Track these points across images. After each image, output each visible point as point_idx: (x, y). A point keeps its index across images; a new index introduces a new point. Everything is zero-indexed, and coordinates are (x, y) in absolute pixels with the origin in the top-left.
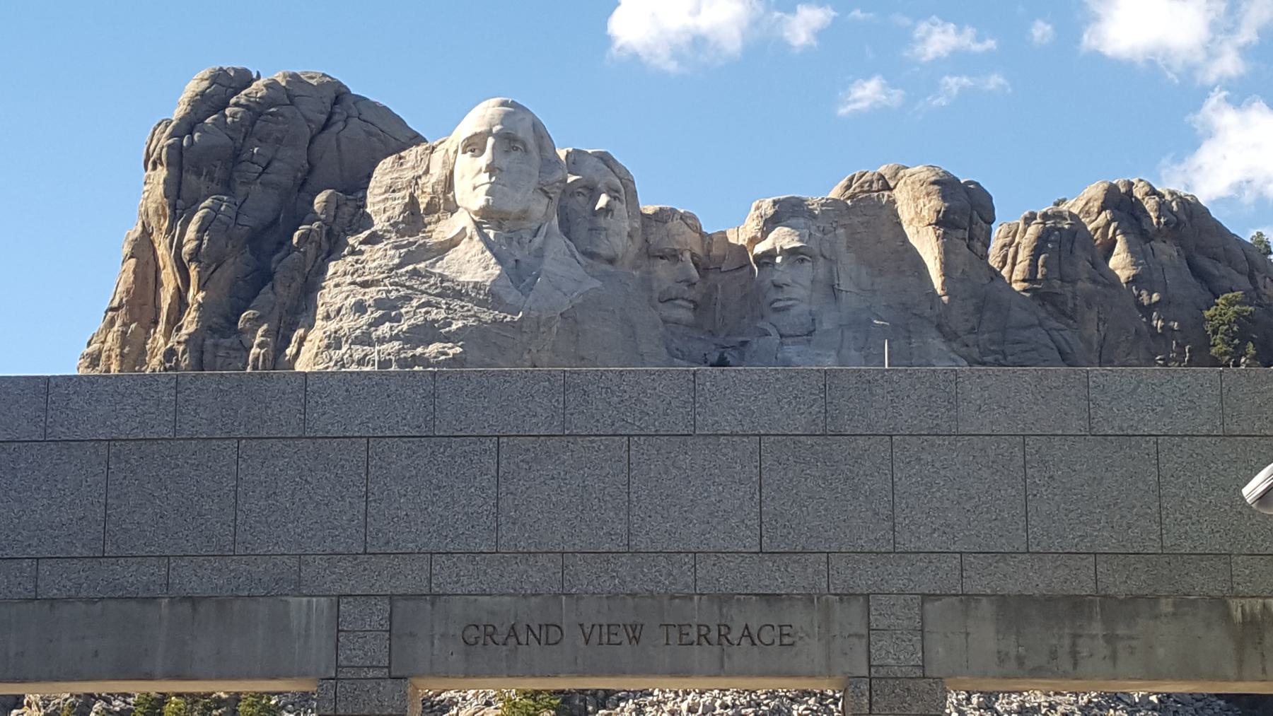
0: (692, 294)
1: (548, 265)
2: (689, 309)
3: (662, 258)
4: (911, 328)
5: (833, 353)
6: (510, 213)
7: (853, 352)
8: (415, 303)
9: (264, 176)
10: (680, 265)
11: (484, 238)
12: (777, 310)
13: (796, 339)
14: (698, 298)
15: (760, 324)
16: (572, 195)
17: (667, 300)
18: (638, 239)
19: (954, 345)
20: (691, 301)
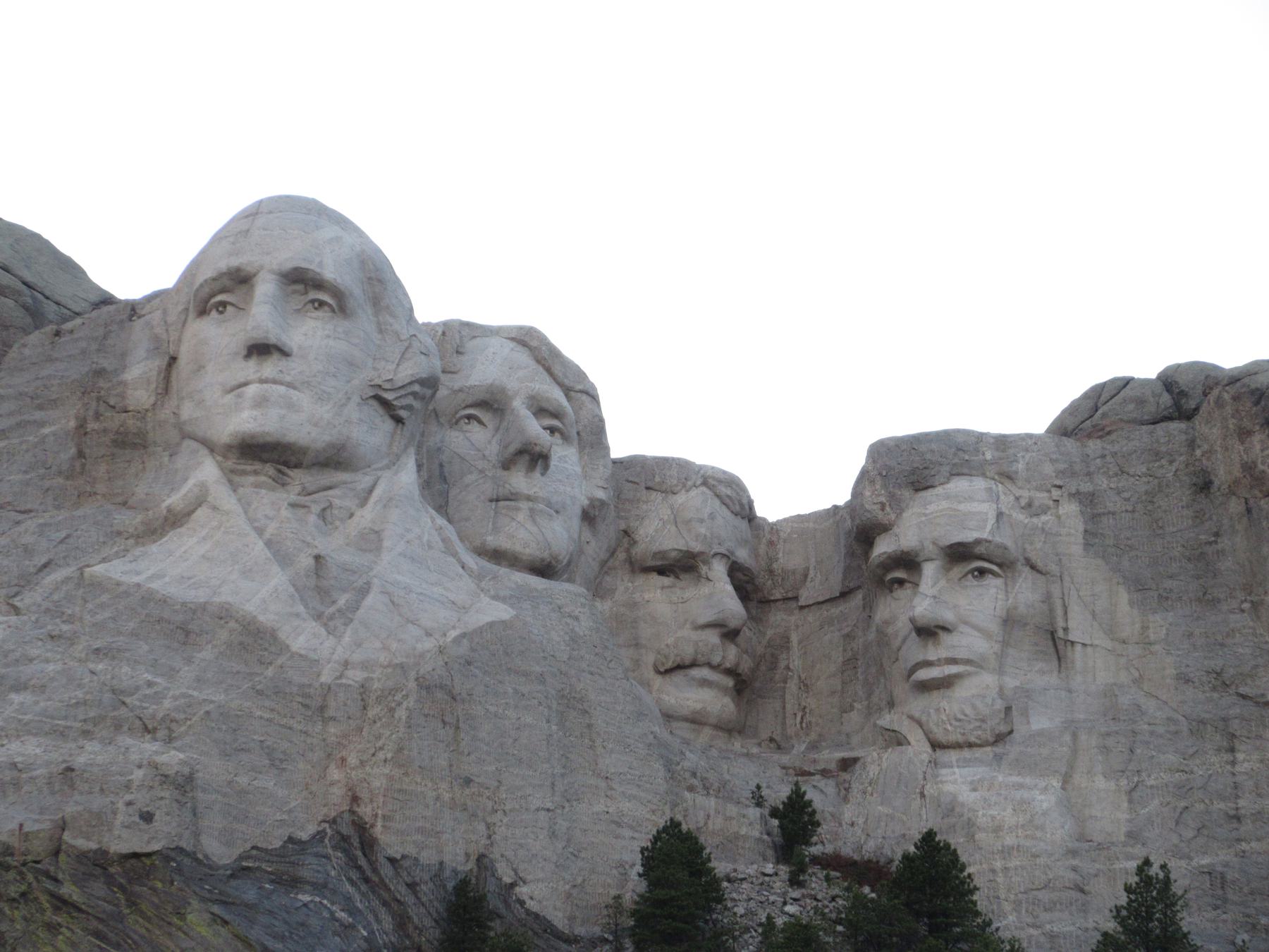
0: (731, 654)
1: (390, 567)
2: (725, 690)
3: (662, 571)
4: (1235, 725)
5: (1056, 783)
6: (303, 451)
7: (1101, 783)
8: (79, 649)
10: (705, 589)
11: (245, 505)
12: (925, 687)
13: (966, 753)
14: (746, 665)
15: (886, 720)
16: (455, 423)
18: (608, 529)
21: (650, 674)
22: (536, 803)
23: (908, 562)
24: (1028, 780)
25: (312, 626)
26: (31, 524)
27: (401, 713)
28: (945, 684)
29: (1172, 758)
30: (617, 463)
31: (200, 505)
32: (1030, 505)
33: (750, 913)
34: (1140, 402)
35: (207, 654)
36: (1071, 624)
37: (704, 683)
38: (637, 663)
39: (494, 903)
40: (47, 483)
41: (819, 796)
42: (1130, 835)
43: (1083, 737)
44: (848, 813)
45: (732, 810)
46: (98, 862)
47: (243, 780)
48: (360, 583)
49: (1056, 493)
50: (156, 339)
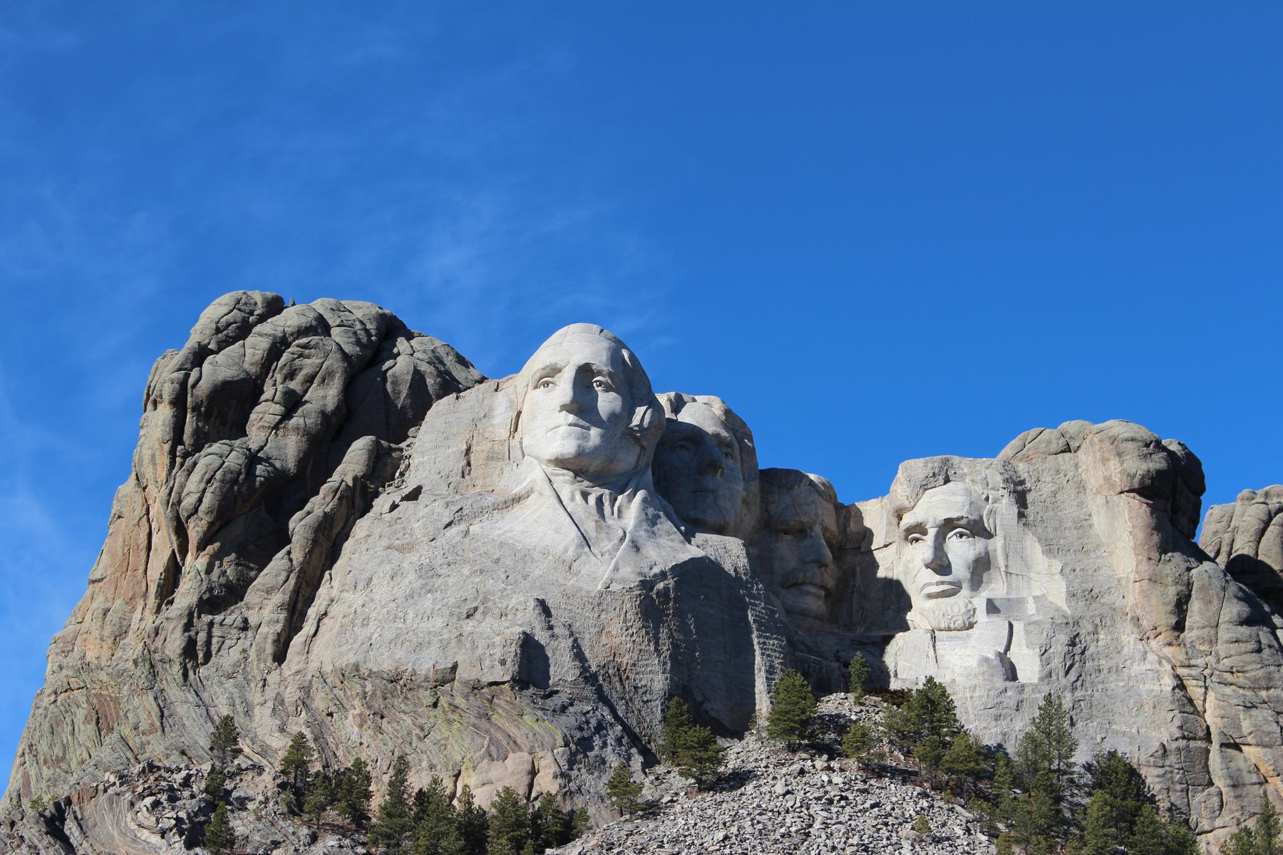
2: (819, 597)
7: (1025, 651)
10: (808, 542)
14: (831, 583)
18: (756, 509)
20: (823, 587)
29: (1063, 638)
32: (987, 499)
34: (1049, 442)
36: (1011, 563)
37: (808, 593)
40: (450, 480)
42: (1042, 679)
46: (476, 687)
48: (621, 533)
49: (1002, 492)
50: (511, 401)
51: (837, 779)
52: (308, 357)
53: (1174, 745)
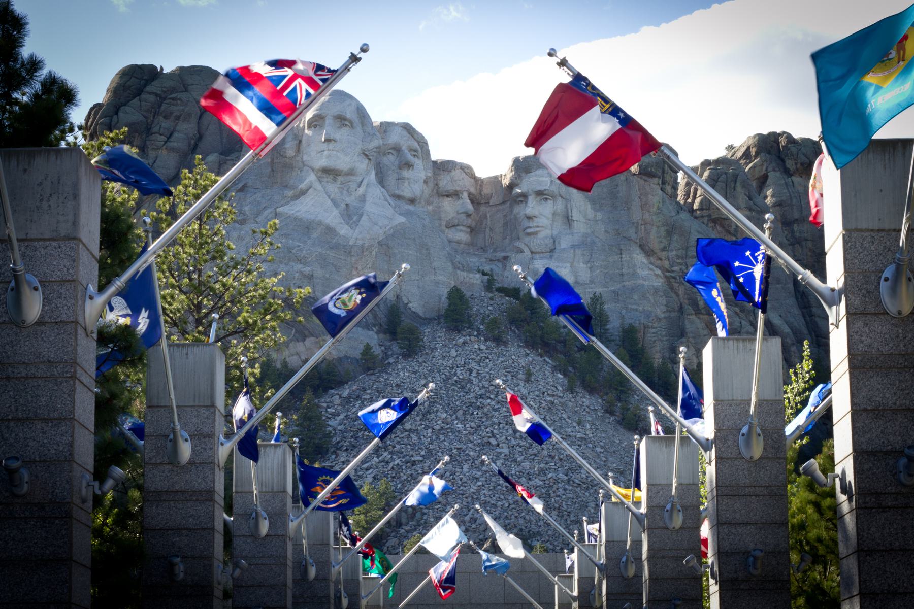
0: (469, 222)
1: (369, 207)
3: (448, 196)
4: (622, 247)
5: (568, 265)
6: (342, 171)
7: (582, 265)
9: (168, 143)
10: (460, 202)
12: (529, 234)
14: (473, 225)
15: (517, 244)
16: (385, 154)
17: (451, 226)
18: (431, 185)
19: (652, 259)
20: (469, 227)
21: (444, 228)
22: (413, 278)
23: (524, 196)
24: (560, 265)
25: (346, 227)
26: (259, 195)
27: (374, 253)
28: (536, 233)
30: (435, 163)
31: (310, 188)
33: (478, 310)
35: (315, 235)
37: (461, 231)
38: (440, 225)
39: (402, 309)
41: (497, 268)
42: (592, 282)
43: (577, 250)
44: (506, 274)
45: (471, 275)
47: (327, 275)
51: (483, 347)
52: (176, 105)
53: (663, 315)
